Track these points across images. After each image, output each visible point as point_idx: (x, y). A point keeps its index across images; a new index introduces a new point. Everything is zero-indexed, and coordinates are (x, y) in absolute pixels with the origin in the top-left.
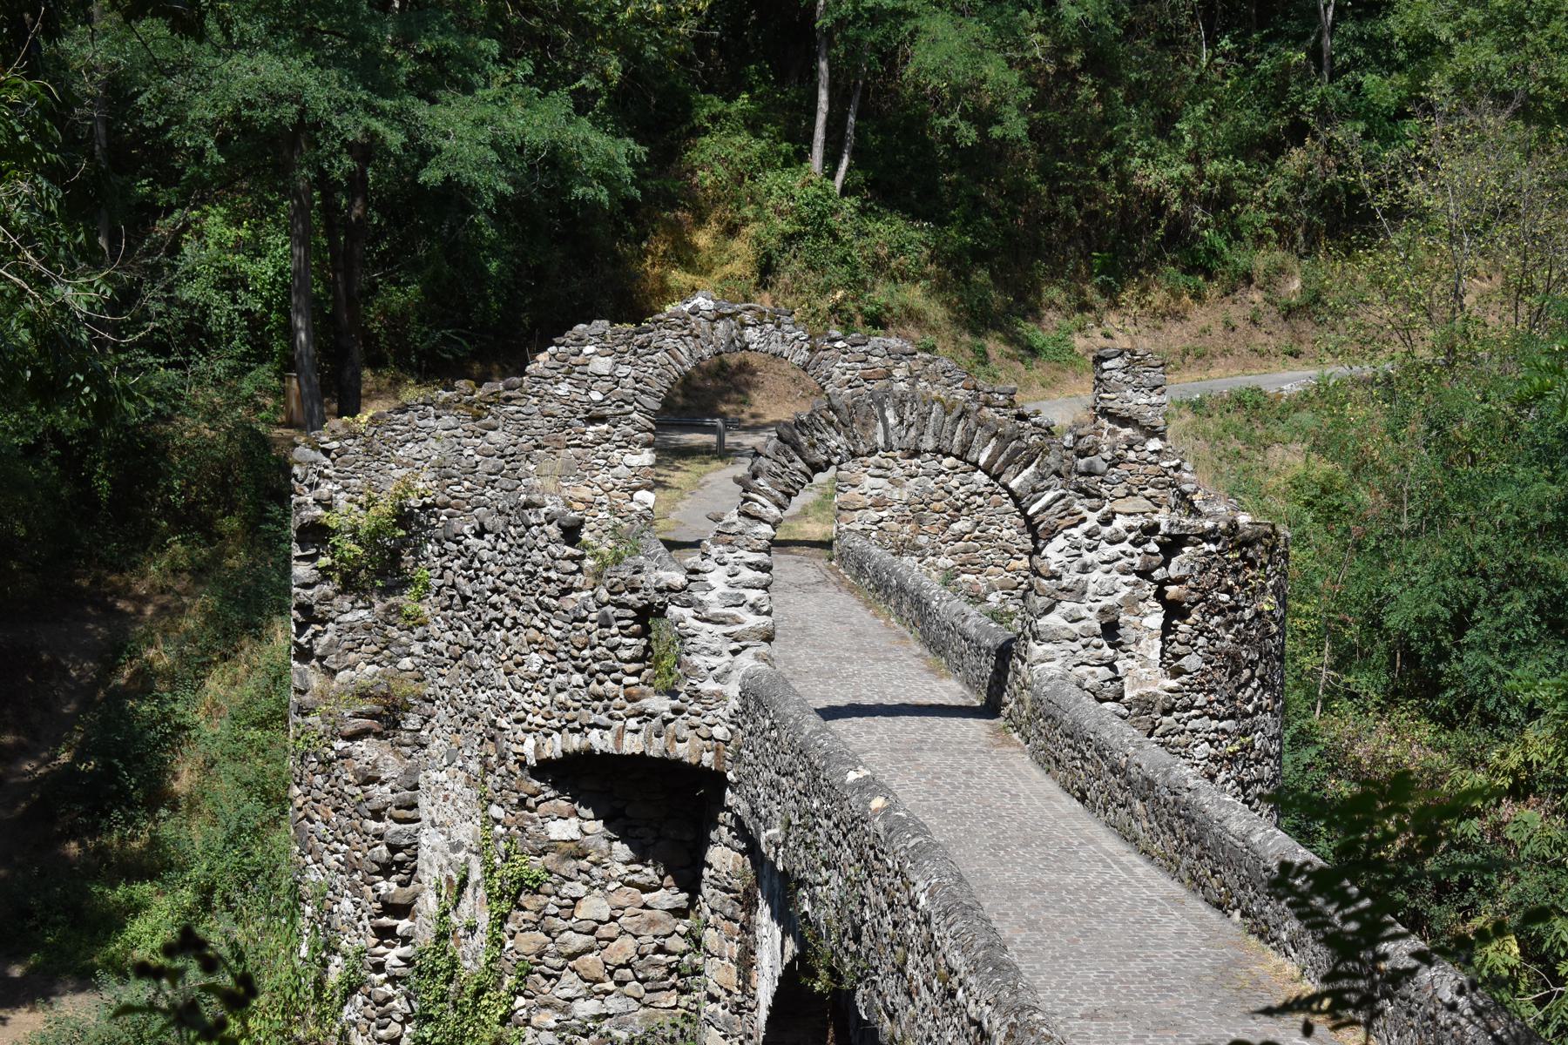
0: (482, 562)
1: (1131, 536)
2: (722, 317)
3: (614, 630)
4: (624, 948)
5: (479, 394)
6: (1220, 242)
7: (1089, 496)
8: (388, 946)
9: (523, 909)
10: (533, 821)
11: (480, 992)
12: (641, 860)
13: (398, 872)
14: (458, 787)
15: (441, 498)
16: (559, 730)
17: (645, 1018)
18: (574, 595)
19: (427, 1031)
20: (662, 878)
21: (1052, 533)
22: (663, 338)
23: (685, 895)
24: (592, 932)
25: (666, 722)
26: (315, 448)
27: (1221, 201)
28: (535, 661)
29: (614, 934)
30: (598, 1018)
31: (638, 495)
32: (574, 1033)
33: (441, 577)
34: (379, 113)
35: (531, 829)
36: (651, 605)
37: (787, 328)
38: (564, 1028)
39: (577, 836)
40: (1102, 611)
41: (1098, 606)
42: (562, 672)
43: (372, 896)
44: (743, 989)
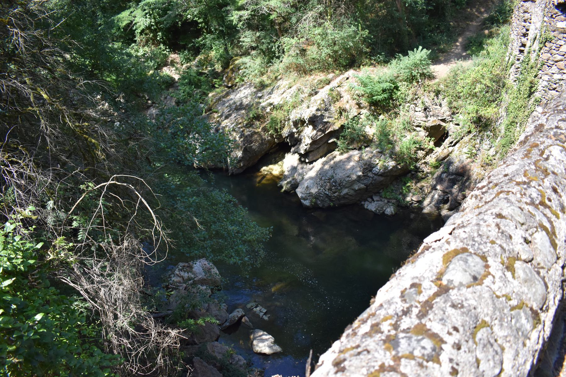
10: (553, 21)
30: (560, 80)
35: (552, 24)
38: (550, 81)
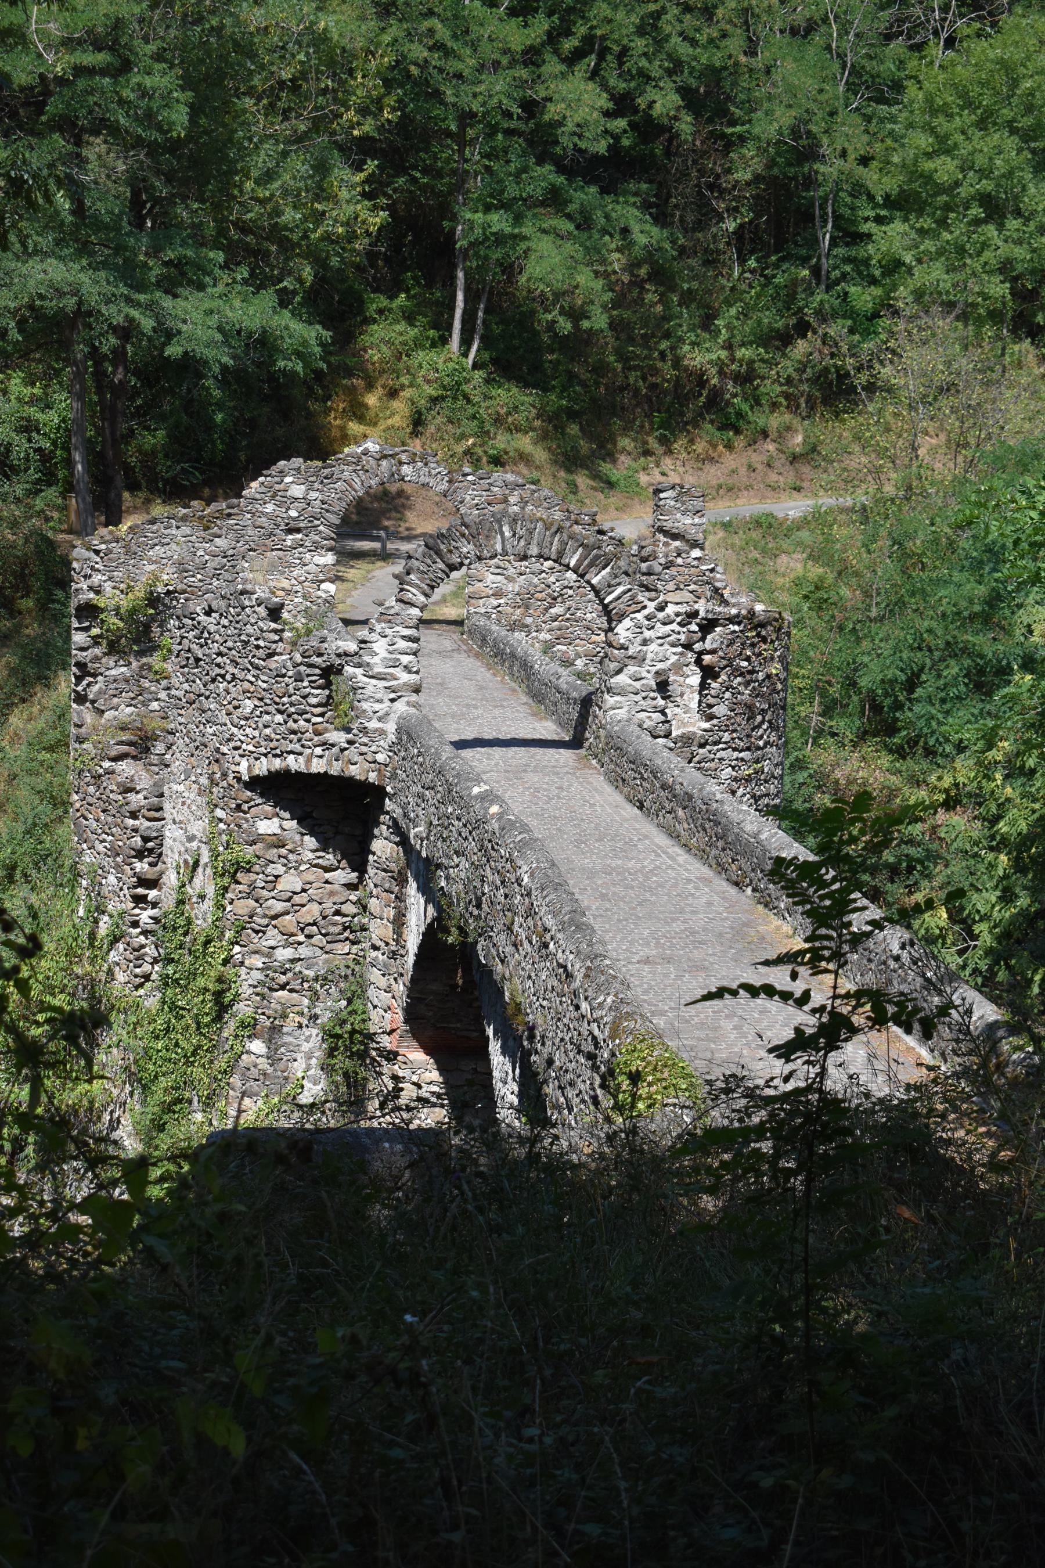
0: (210, 633)
1: (679, 619)
2: (385, 457)
3: (306, 684)
4: (313, 911)
5: (208, 511)
6: (745, 407)
7: (648, 590)
8: (142, 909)
9: (239, 883)
11: (207, 942)
12: (324, 849)
13: (149, 856)
14: (192, 796)
15: (180, 587)
16: (265, 755)
17: (326, 961)
18: (276, 658)
19: (170, 970)
20: (339, 862)
21: (622, 617)
22: (343, 471)
23: (355, 874)
24: (289, 900)
25: (343, 750)
26: (88, 549)
27: (746, 378)
28: (248, 705)
29: (304, 901)
30: (293, 961)
31: (323, 586)
32: (275, 972)
33: (180, 644)
34: (137, 305)
35: (245, 826)
36: (332, 665)
37: (432, 465)
38: (268, 968)
39: (278, 831)
40: (657, 673)
41: (654, 669)
42: (267, 713)
43: (130, 873)
44: (397, 941)
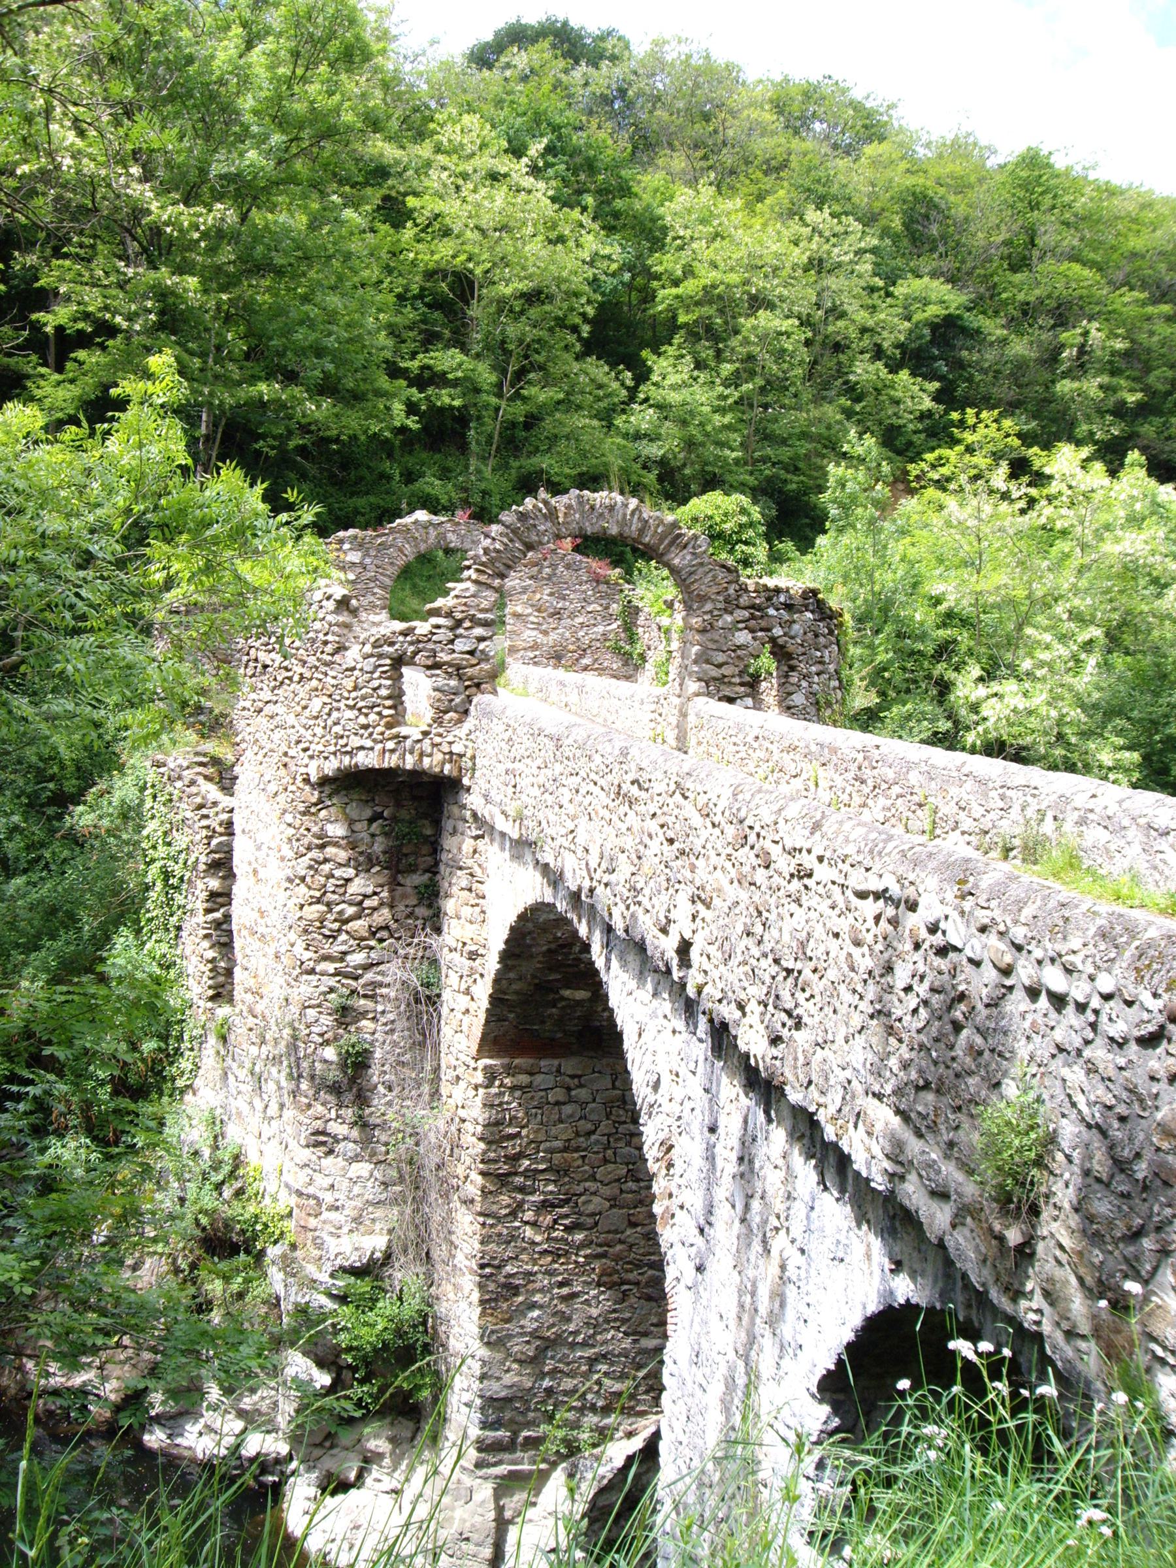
16: (335, 754)
42: (338, 709)
